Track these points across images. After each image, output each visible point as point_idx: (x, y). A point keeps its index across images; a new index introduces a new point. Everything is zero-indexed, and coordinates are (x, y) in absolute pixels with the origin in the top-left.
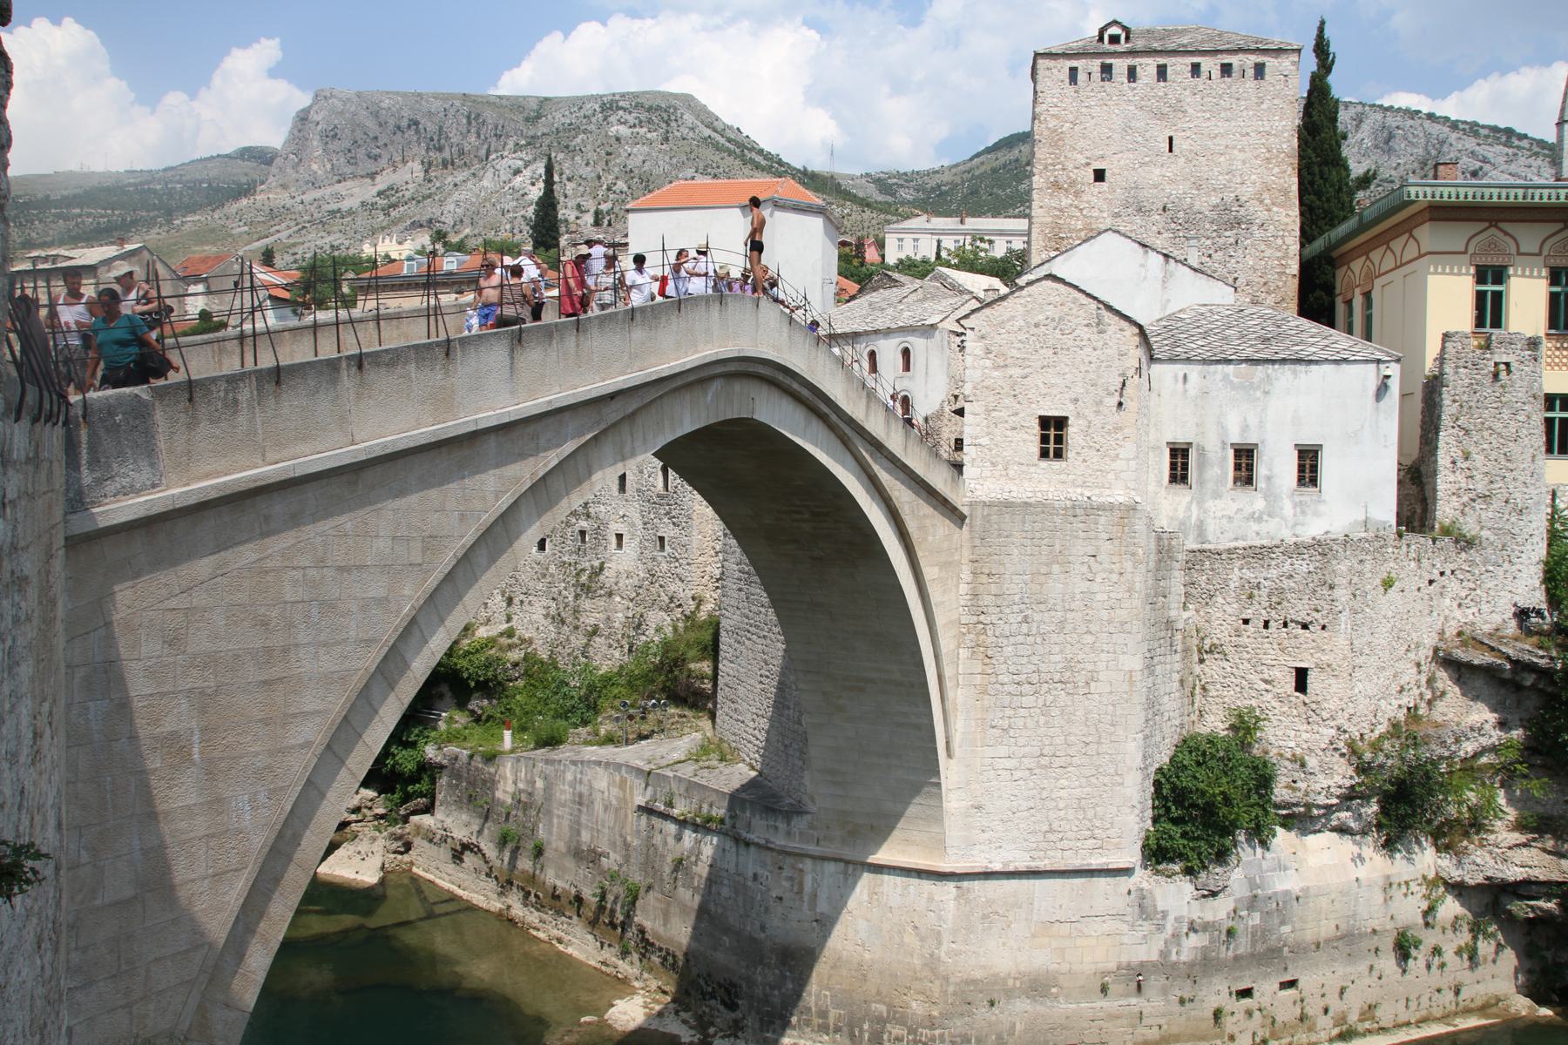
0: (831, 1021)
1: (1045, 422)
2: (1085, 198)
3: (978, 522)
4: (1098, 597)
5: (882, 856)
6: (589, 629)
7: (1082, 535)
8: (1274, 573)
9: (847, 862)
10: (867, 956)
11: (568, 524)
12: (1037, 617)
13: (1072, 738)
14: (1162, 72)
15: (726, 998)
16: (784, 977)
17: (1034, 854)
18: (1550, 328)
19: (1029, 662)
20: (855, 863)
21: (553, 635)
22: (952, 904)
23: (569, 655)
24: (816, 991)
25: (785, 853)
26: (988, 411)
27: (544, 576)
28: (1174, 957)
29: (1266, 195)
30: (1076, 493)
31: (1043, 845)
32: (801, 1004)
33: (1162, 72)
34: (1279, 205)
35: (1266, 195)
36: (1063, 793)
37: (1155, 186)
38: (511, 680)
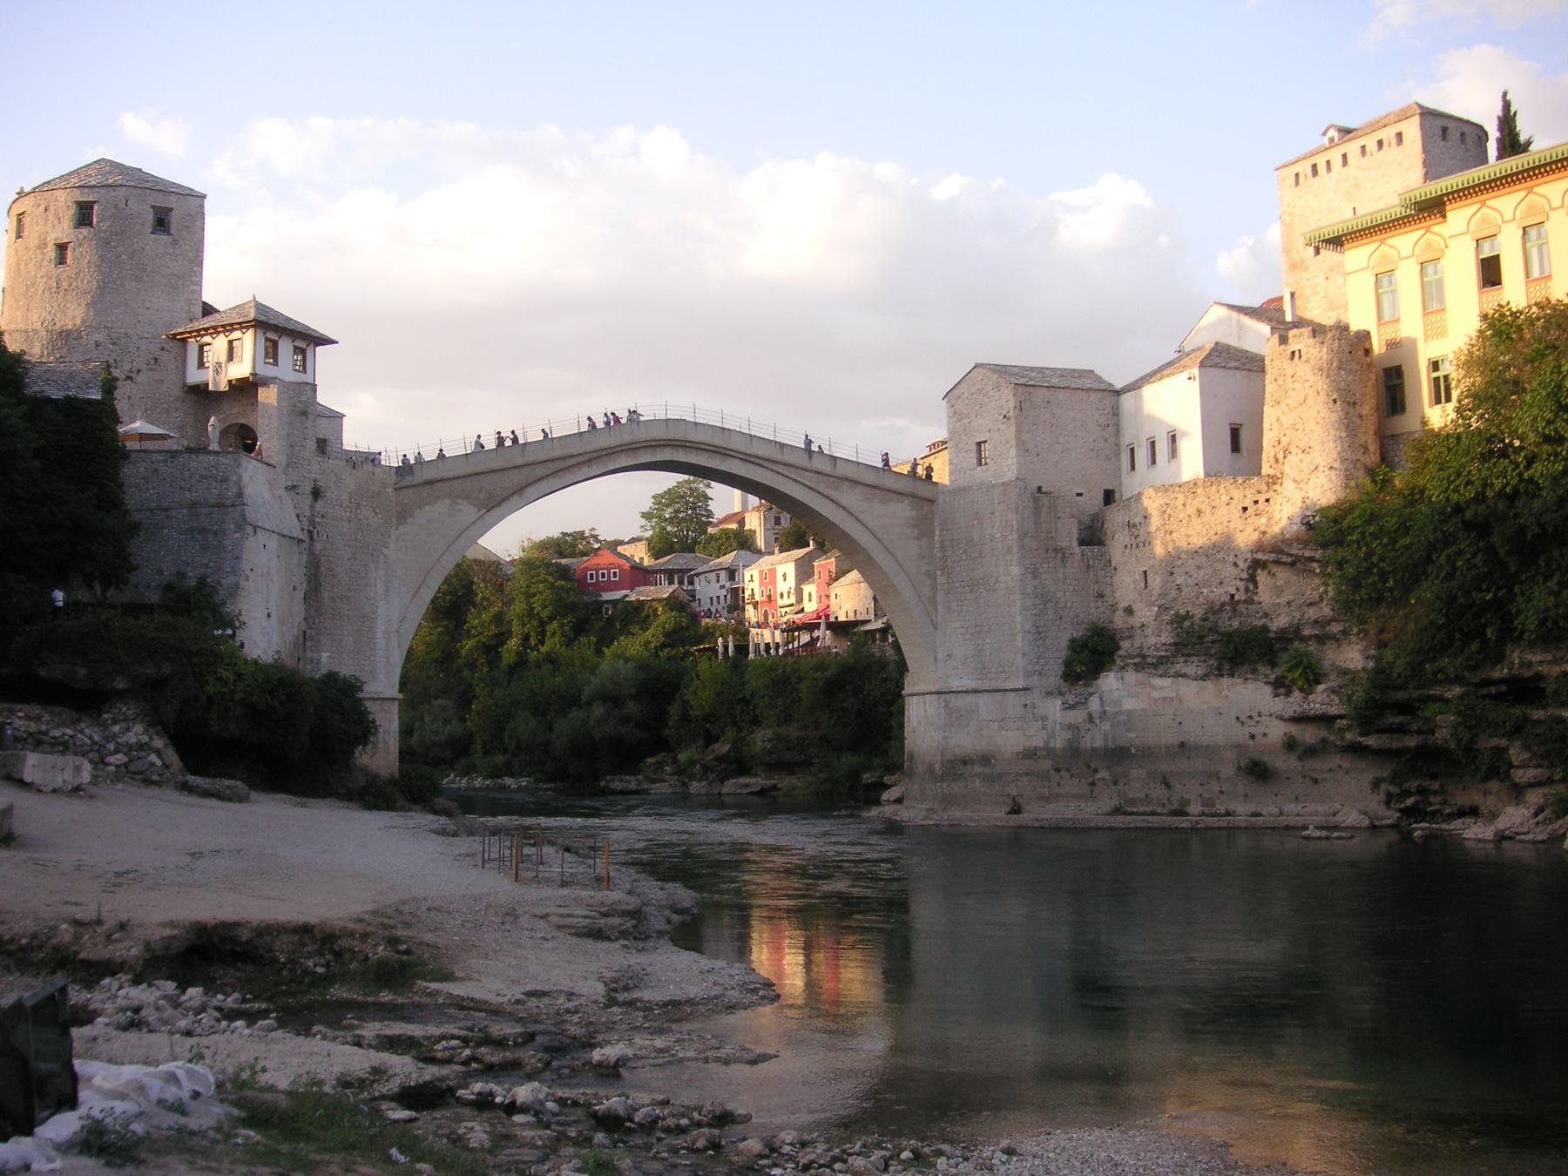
4: (998, 535)
12: (970, 550)
28: (1052, 744)
36: (988, 647)
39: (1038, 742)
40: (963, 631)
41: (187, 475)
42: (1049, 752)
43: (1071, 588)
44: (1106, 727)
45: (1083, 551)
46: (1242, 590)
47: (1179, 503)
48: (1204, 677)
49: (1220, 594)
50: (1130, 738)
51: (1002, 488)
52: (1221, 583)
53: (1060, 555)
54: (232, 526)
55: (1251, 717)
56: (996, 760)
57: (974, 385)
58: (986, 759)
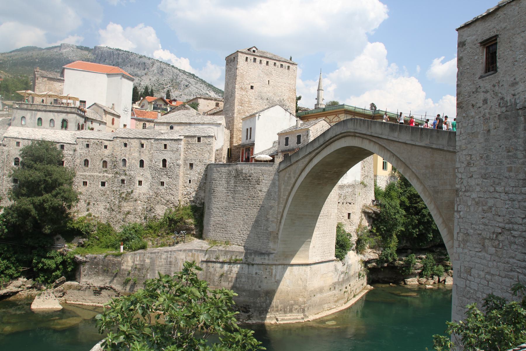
0: (279, 308)
5: (293, 262)
6: (126, 212)
8: (344, 191)
9: (284, 265)
10: (289, 289)
11: (115, 177)
14: (267, 62)
15: (245, 310)
16: (266, 299)
17: (322, 258)
20: (286, 265)
21: (108, 215)
22: (309, 272)
23: (116, 221)
24: (276, 301)
25: (268, 265)
27: (105, 195)
29: (289, 99)
31: (323, 255)
32: (271, 305)
33: (267, 62)
34: (292, 103)
35: (289, 99)
36: (326, 243)
37: (265, 93)
38: (92, 231)
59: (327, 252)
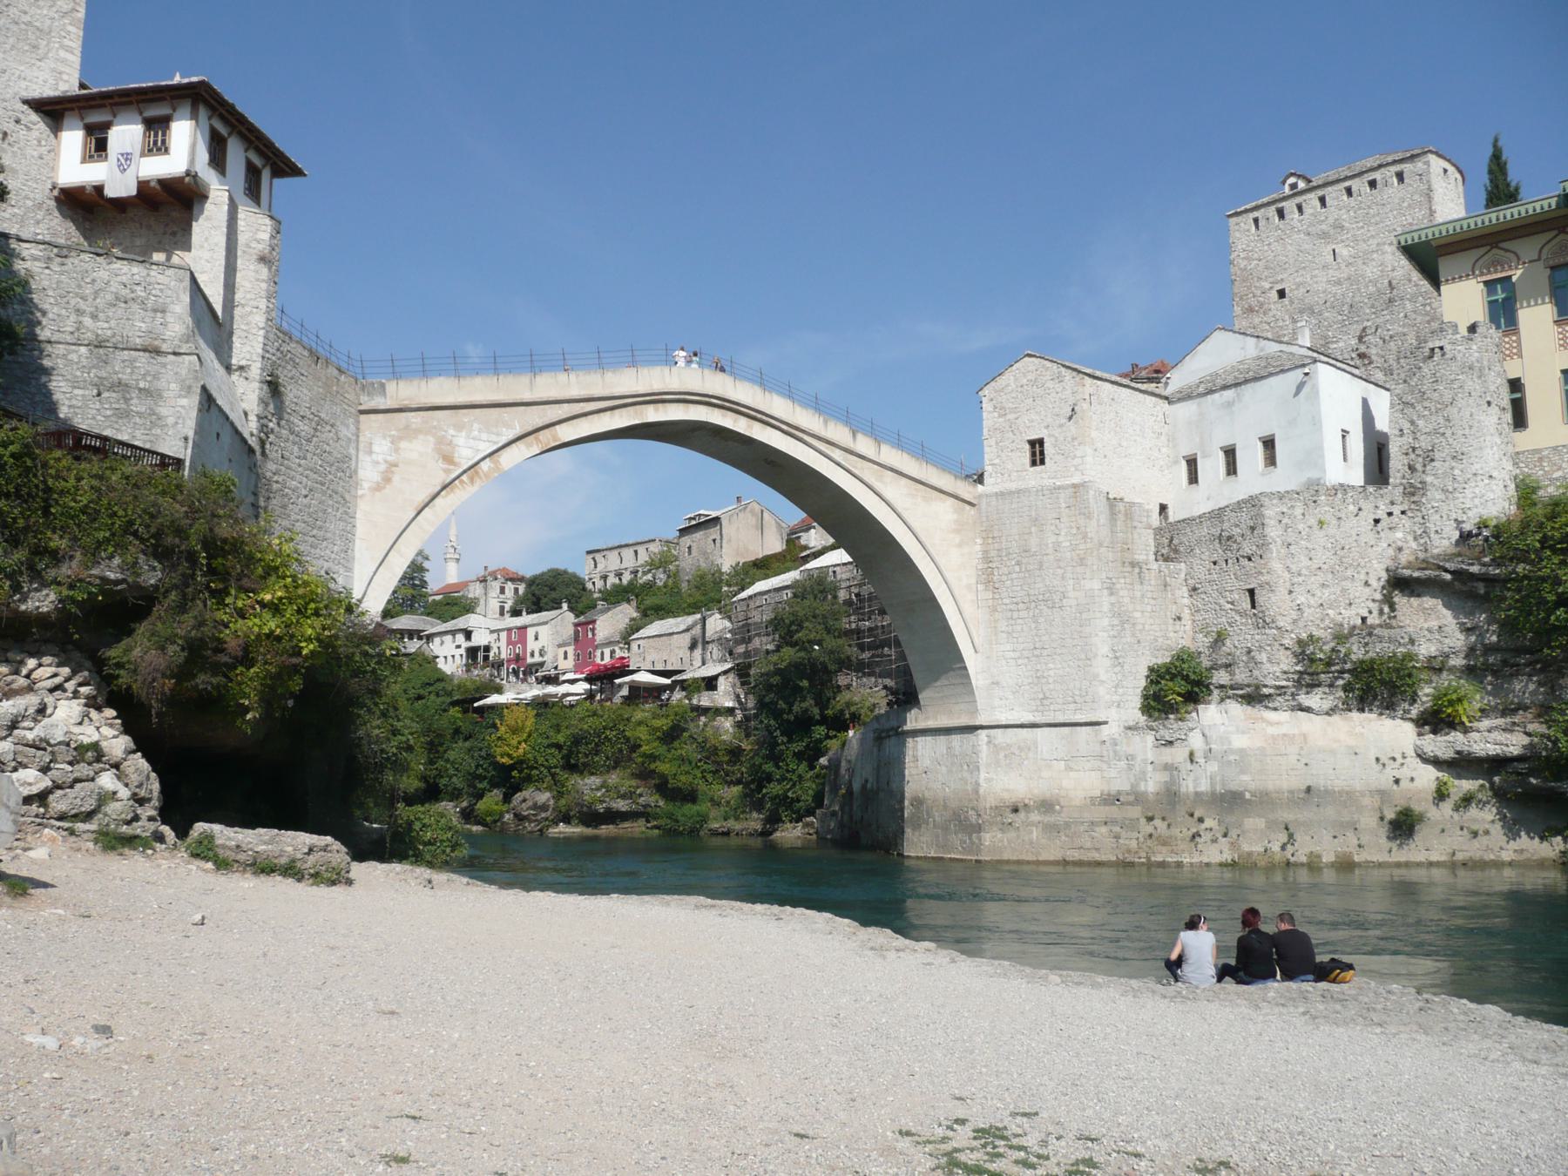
1: (1032, 443)
2: (1271, 314)
3: (984, 506)
4: (1064, 544)
7: (1049, 506)
12: (1024, 561)
13: (1054, 636)
14: (1322, 200)
18: (1559, 316)
19: (1022, 590)
26: (997, 443)
28: (1142, 788)
30: (1048, 482)
31: (1041, 708)
33: (1322, 200)
36: (1051, 673)
39: (1121, 784)
40: (1012, 654)
41: (88, 291)
42: (1138, 798)
43: (1149, 608)
44: (1213, 767)
45: (1160, 566)
46: (1375, 613)
47: (1298, 511)
48: (1331, 712)
49: (1351, 617)
50: (1245, 781)
51: (1071, 490)
52: (1351, 604)
53: (1137, 570)
54: (173, 386)
55: (1394, 759)
56: (1062, 807)
57: (1025, 376)
58: (1046, 806)
59: (1060, 701)
